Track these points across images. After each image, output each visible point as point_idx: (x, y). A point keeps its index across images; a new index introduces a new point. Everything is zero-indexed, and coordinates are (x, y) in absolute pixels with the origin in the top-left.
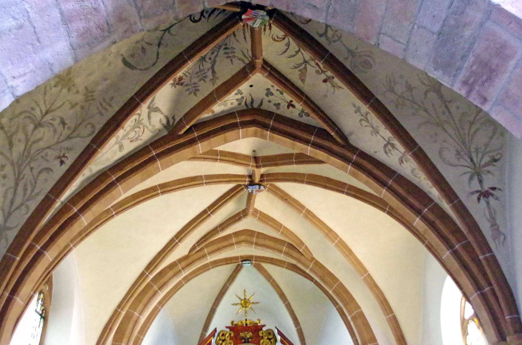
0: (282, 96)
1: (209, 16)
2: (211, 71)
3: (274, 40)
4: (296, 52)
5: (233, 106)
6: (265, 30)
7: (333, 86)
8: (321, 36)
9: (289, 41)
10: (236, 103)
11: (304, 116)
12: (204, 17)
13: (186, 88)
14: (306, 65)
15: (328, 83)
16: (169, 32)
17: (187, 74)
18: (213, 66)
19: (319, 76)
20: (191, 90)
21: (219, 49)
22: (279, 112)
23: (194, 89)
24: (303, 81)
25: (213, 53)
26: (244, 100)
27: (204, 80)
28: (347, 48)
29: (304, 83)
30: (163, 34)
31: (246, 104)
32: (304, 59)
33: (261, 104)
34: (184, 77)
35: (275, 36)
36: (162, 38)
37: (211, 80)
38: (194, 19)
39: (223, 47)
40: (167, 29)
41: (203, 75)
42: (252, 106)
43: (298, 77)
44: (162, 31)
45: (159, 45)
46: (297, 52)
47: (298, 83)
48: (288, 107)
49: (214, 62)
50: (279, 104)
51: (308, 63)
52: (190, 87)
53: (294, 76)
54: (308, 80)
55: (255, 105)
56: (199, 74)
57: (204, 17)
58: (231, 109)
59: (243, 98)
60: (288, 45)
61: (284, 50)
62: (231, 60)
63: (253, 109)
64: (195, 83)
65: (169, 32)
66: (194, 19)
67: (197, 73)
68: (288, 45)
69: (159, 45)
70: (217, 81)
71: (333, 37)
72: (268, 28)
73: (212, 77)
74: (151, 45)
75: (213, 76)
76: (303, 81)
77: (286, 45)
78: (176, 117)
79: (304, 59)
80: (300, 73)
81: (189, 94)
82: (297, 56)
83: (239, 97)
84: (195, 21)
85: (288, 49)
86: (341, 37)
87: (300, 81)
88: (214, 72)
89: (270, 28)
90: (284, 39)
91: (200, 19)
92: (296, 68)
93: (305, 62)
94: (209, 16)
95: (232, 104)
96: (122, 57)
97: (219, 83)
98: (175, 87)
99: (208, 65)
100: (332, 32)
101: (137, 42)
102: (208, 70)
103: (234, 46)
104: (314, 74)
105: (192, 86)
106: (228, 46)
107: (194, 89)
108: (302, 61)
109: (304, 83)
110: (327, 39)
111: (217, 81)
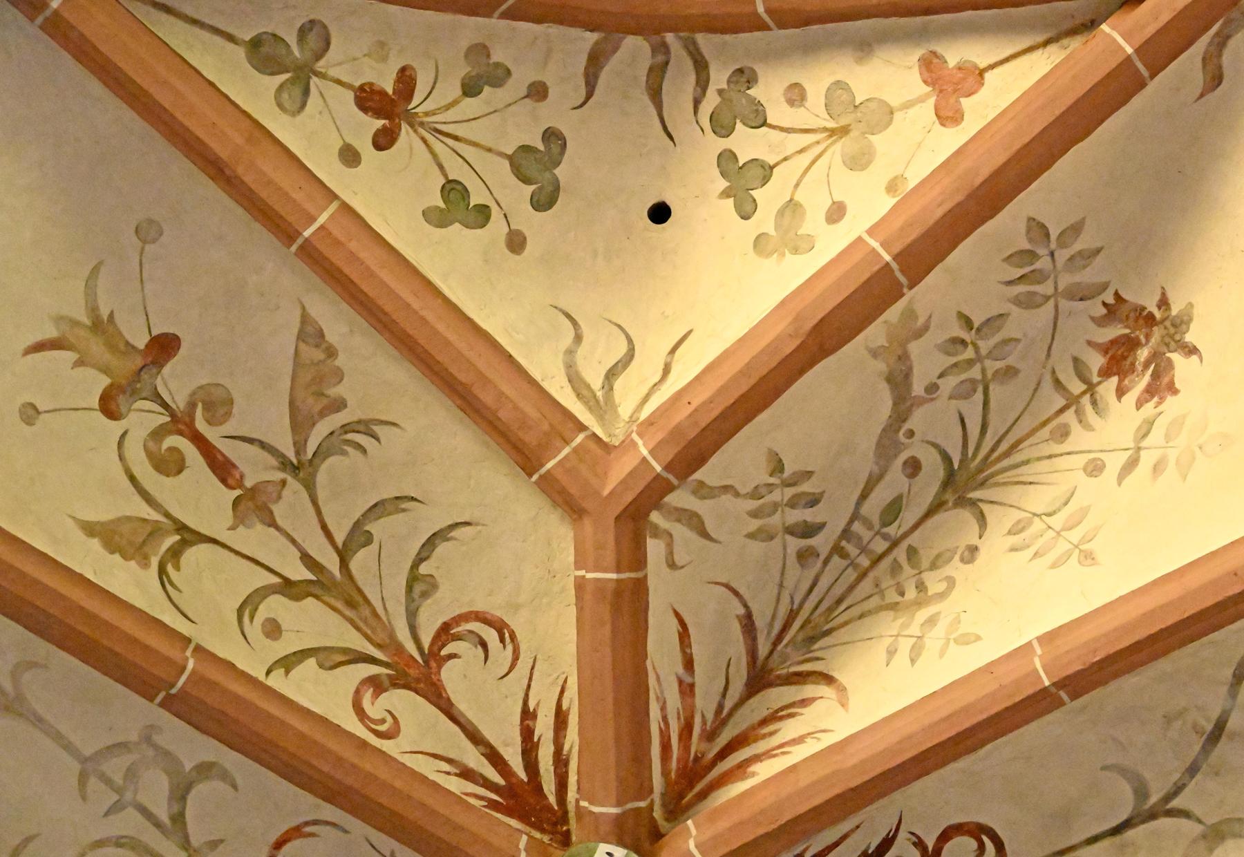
0: (457, 171)
2: (918, 389)
3: (500, 627)
4: (368, 539)
5: (791, 75)
7: (102, 326)
8: (205, 770)
9: (412, 616)
10: (769, 91)
11: (292, 40)
12: (919, 844)
13: (1088, 276)
14: (300, 447)
15: (141, 342)
16: (1141, 792)
17: (1077, 387)
18: (900, 416)
20: (1062, 256)
21: (846, 533)
22: (471, 28)
23: (1043, 263)
24: (310, 333)
25: (893, 510)
26: (711, 101)
27: (967, 322)
28: (38, 721)
29: (305, 318)
30: (1177, 790)
31: (701, 66)
32: (310, 487)
33: (595, 62)
34: (1096, 361)
35: (501, 655)
36: (1193, 770)
37: (919, 334)
38: (982, 846)
39: (821, 542)
40: (1152, 816)
41: (969, 353)
42: (663, 48)
43: (340, 361)
44: (1185, 814)
45: (1218, 732)
46: (359, 536)
48: (406, 80)
49: (888, 444)
50: (470, 89)
51: (285, 464)
52: (1065, 281)
53: (372, 375)
54: (282, 343)
55: (634, 51)
56: (992, 366)
57: (919, 844)
58: (810, 50)
59: (722, 127)
61: (442, 549)
62: (778, 466)
63: (651, 27)
64: (1028, 302)
65: (1141, 792)
67: (1010, 373)
68: (418, 586)
69: (1218, 732)
70: (882, 341)
71: (131, 774)
72: (544, 727)
73: (914, 348)
75: (904, 357)
76: (310, 333)
77: (432, 585)
78: (1198, 79)
79: (310, 487)
80: (334, 392)
81: (1076, 229)
83: (748, 144)
84: (979, 831)
85: (420, 559)
86: (83, 778)
88: (899, 381)
89: (528, 715)
90: (445, 632)
92: (366, 427)
93: (301, 469)
95: (796, 96)
97: (875, 334)
98: (1164, 303)
99: (935, 425)
100: (143, 799)
102: (932, 388)
103: (757, 547)
104: (238, 388)
105: (1046, 288)
106: (794, 544)
107: (1043, 263)
108: (322, 478)
109: (305, 318)
110: (167, 758)
111: (882, 341)
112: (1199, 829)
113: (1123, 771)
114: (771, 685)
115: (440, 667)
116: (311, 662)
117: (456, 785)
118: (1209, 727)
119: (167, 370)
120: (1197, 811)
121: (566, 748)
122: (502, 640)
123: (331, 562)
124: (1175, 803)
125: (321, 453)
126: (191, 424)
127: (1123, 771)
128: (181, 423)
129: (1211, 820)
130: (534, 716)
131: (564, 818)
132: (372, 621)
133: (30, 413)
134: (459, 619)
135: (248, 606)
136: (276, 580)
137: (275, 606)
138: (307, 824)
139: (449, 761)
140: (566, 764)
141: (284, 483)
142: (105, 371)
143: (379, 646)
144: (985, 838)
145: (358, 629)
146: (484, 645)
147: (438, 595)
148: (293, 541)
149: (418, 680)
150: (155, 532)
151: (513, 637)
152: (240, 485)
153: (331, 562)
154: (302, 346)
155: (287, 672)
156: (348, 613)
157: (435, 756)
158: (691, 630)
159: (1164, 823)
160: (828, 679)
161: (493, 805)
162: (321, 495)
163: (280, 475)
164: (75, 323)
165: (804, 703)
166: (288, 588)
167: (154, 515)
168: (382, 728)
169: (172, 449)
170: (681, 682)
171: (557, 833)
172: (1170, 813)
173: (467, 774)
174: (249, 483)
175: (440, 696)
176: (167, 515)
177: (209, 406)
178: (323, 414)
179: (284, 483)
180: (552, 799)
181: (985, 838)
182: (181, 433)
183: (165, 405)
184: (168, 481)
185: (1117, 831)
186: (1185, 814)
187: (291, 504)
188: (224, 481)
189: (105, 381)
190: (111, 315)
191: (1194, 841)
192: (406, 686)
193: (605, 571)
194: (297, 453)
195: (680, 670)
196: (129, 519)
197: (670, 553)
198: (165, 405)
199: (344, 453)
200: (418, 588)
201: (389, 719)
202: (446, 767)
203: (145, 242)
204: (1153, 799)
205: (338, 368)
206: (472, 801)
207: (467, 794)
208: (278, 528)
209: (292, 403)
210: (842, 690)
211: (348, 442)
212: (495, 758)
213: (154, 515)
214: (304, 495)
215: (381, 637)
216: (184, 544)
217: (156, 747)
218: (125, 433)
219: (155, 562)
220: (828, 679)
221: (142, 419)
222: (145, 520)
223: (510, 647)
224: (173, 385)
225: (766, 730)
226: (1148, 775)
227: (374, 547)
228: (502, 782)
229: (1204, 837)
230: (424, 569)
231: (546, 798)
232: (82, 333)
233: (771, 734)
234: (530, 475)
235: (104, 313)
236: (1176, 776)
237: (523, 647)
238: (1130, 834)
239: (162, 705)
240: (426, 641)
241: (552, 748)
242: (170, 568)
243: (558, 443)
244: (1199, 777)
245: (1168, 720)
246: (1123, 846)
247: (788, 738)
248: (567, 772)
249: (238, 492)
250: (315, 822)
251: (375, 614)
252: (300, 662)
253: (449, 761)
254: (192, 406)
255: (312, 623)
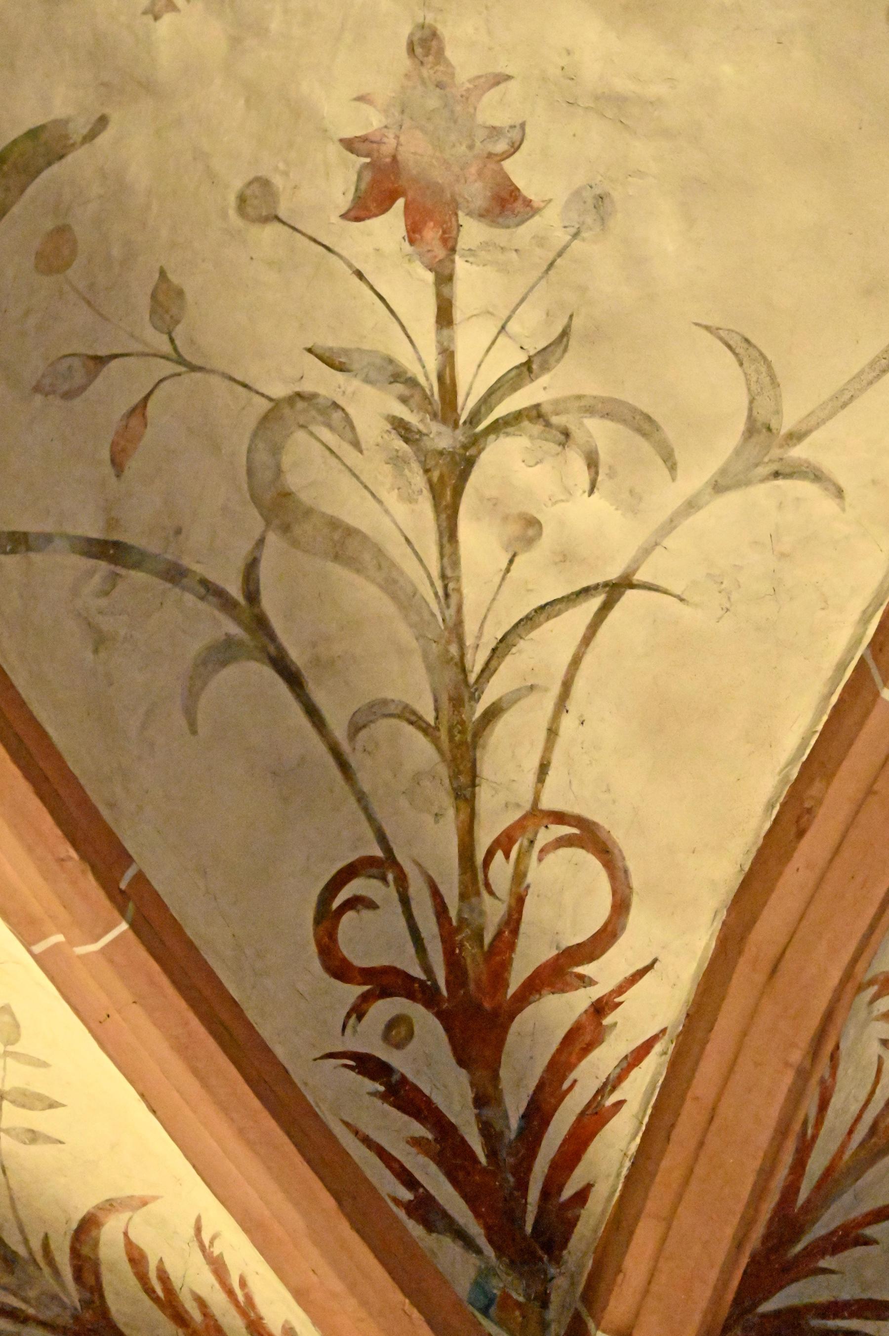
1: (366, 1065)
12: (358, 1011)
16: (224, 653)
36: (175, 574)
38: (353, 903)
40: (260, 624)
45: (110, 551)
57: (358, 1011)
65: (224, 653)
66: (353, 903)
69: (110, 551)
74: (117, 463)
84: (327, 917)
91: (339, 969)
94: (366, 1065)
96: (80, 127)
101: (166, 302)
112: (272, 538)
113: (192, 695)
114: (104, 1313)
118: (103, 566)
120: (243, 549)
124: (235, 590)
127: (192, 695)
129: (255, 521)
144: (336, 904)
159: (269, 604)
160: (87, 1226)
165: (136, 1258)
172: (252, 596)
181: (336, 904)
185: (293, 679)
186: (250, 573)
191: (295, 543)
204: (233, 629)
210: (110, 1206)
220: (87, 1226)
225: (196, 1315)
226: (195, 647)
229: (286, 528)
233: (202, 1303)
236: (189, 599)
238: (296, 655)
244: (187, 562)
245: (100, 641)
246: (316, 661)
247: (211, 1279)
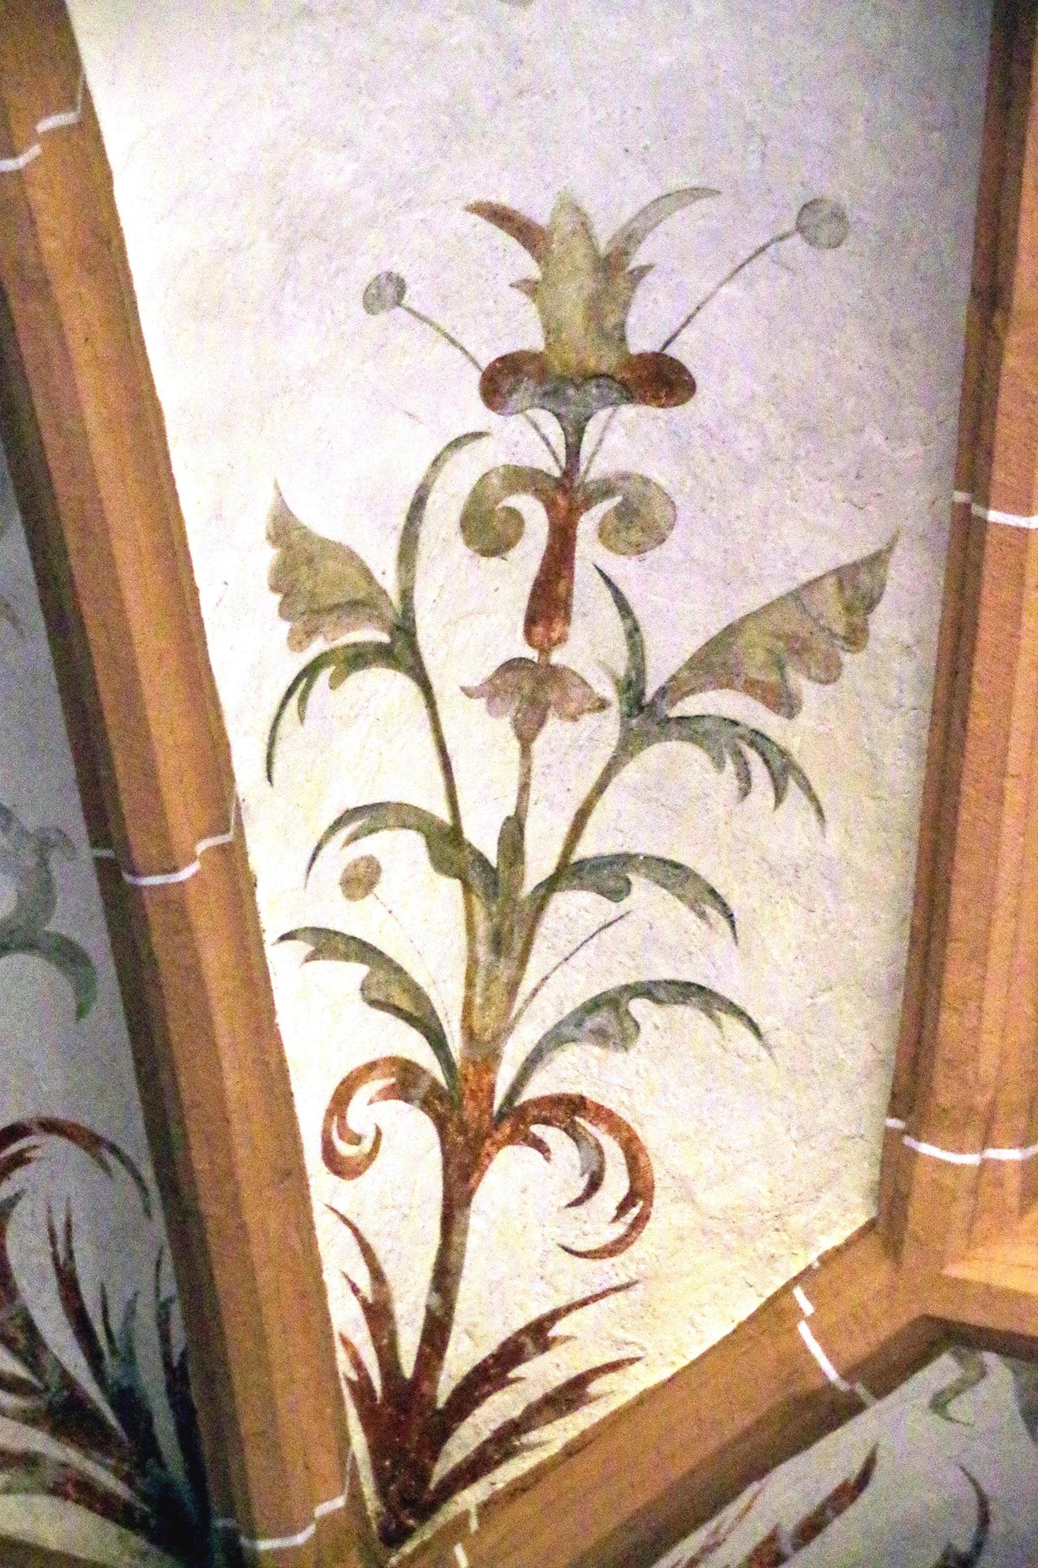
6: (571, 1395)
19: (661, 472)
46: (609, 875)
47: (904, 619)
60: (606, 1018)
72: (540, 1374)
76: (858, 586)
82: (644, 845)
87: (887, 623)
115: (510, 1140)
116: (358, 971)
117: (346, 1316)
119: (629, 412)
121: (533, 1436)
122: (623, 1208)
123: (540, 861)
125: (689, 728)
126: (574, 512)
128: (566, 494)
130: (544, 1345)
131: (426, 1510)
132: (498, 991)
133: (387, 293)
134: (604, 1116)
135: (371, 816)
136: (443, 814)
137: (402, 852)
138: (114, 1149)
139: (377, 1276)
140: (510, 1454)
141: (603, 705)
142: (551, 330)
143: (470, 1035)
145: (470, 984)
146: (594, 1184)
147: (618, 1058)
148: (524, 788)
149: (463, 1128)
150: (363, 604)
151: (639, 1223)
152: (544, 651)
153: (540, 861)
154: (830, 586)
155: (311, 957)
156: (483, 951)
157: (367, 1251)
158: (865, 1498)
161: (362, 1390)
162: (630, 773)
163: (607, 690)
164: (585, 228)
166: (447, 845)
167: (389, 582)
168: (344, 1149)
169: (514, 515)
170: (772, 1538)
171: (397, 1517)
173: (379, 1314)
174: (557, 658)
175: (466, 1177)
176: (406, 595)
177: (627, 513)
178: (751, 687)
179: (603, 705)
180: (441, 1470)
182: (550, 506)
183: (573, 451)
184: (459, 549)
187: (576, 744)
188: (531, 621)
189: (534, 341)
190: (643, 271)
192: (441, 1123)
193: (830, 1354)
194: (662, 692)
195: (789, 1526)
196: (352, 556)
197: (956, 1391)
198: (573, 451)
199: (720, 765)
200: (601, 1018)
201: (367, 1146)
202: (363, 1280)
203: (800, 229)
205: (840, 666)
206: (342, 1359)
207: (345, 1342)
208: (526, 751)
209: (732, 630)
211: (738, 754)
212: (437, 1331)
213: (389, 582)
214: (606, 752)
215: (485, 1021)
216: (384, 655)
217: (43, 863)
218: (478, 435)
219: (318, 646)
221: (528, 438)
222: (367, 575)
223: (620, 1229)
224: (614, 439)
227: (610, 909)
228: (408, 1370)
230: (638, 1007)
231: (435, 1459)
232: (580, 255)
234: (893, 1113)
235: (639, 259)
237: (636, 1250)
239: (99, 862)
240: (532, 1091)
241: (516, 1413)
242: (325, 675)
243: (972, 1136)
248: (498, 1464)
249: (532, 654)
250: (124, 1160)
251: (512, 988)
252: (346, 957)
253: (377, 1276)
254: (606, 490)
255: (424, 922)
